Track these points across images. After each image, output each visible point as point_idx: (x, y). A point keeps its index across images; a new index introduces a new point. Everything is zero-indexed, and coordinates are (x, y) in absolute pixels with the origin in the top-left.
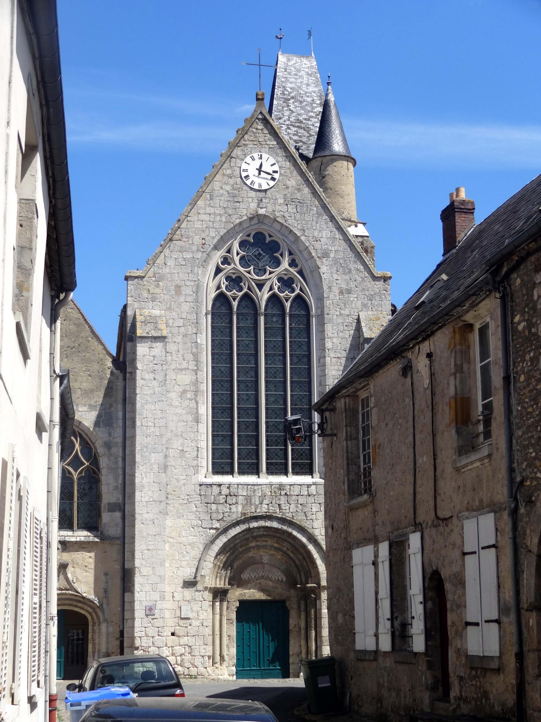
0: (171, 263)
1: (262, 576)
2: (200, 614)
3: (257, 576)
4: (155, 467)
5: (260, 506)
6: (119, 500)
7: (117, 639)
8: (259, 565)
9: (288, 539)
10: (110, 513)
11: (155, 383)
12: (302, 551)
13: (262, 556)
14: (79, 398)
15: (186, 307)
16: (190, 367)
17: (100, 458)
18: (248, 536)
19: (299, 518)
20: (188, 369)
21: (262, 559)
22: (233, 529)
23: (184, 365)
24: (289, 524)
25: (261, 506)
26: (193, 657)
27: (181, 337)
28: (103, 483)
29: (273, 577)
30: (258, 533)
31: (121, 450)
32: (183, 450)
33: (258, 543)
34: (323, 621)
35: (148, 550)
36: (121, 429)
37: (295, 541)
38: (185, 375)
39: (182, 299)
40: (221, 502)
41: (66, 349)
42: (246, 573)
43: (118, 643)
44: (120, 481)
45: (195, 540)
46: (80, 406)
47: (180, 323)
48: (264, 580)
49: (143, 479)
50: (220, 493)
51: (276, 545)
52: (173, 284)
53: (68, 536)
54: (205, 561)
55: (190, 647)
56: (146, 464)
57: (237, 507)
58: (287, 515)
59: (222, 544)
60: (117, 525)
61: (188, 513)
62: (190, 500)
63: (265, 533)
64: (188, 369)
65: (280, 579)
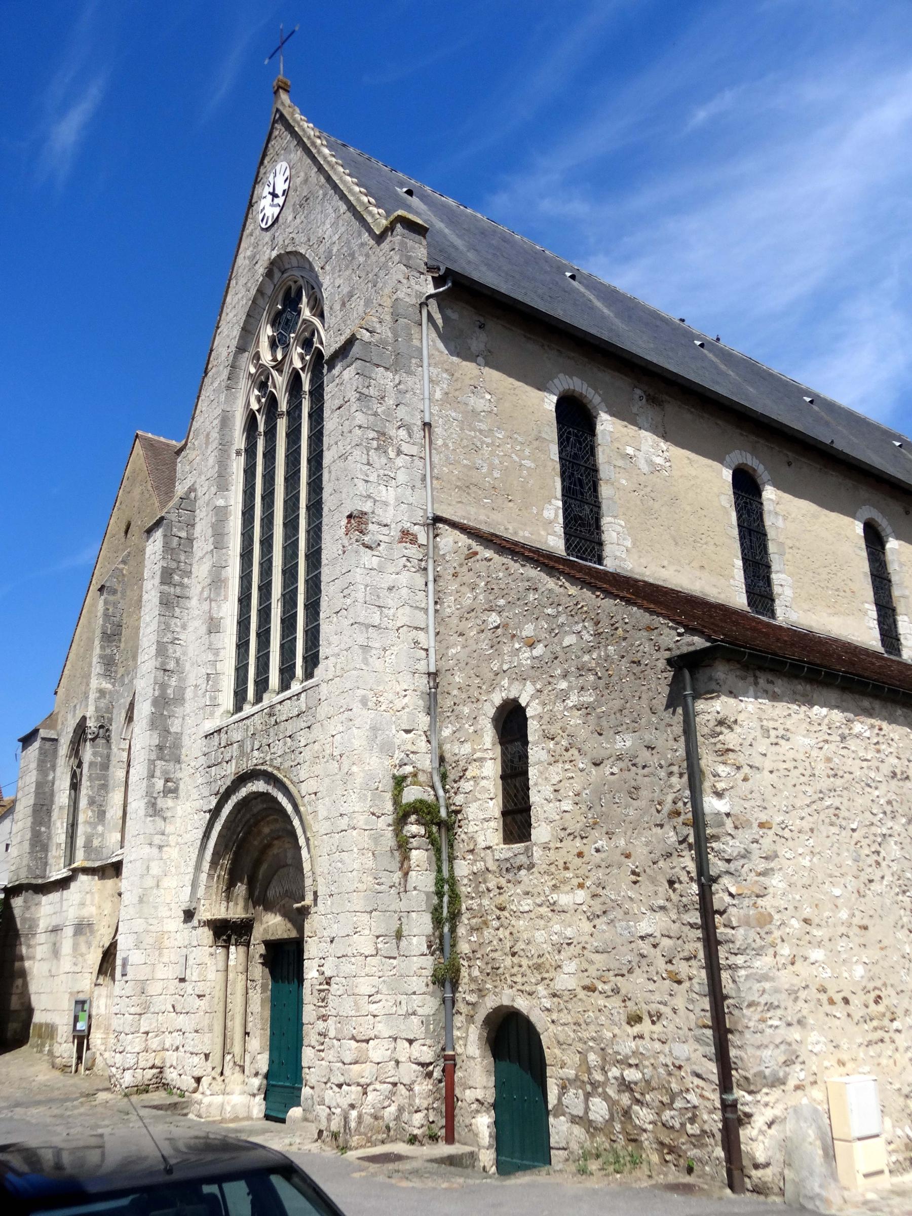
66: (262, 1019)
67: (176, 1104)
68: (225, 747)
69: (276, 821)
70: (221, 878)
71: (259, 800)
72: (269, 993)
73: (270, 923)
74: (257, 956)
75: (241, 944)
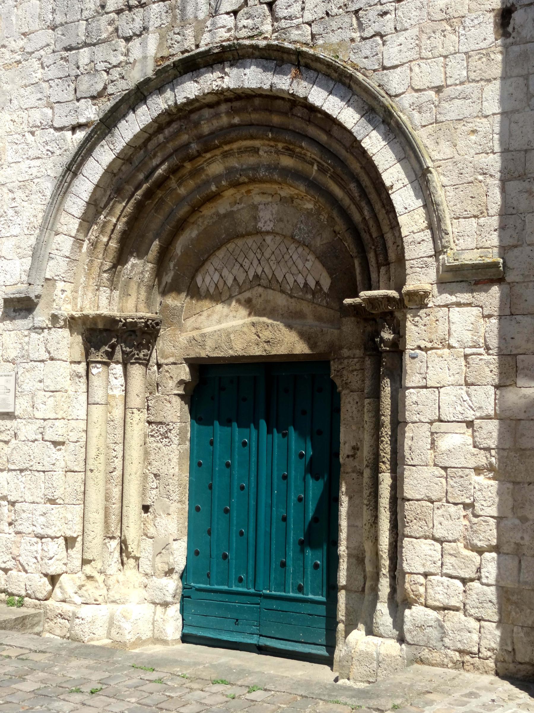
1: (257, 277)
2: (38, 401)
3: (241, 279)
5: (208, 23)
8: (250, 241)
9: (312, 131)
12: (355, 166)
13: (255, 207)
18: (185, 138)
19: (334, 39)
21: (256, 219)
22: (131, 116)
24: (298, 66)
25: (214, 24)
26: (18, 538)
29: (291, 279)
30: (216, 124)
33: (233, 162)
34: (408, 434)
37: (328, 133)
40: (104, 36)
42: (211, 269)
45: (34, 171)
48: (260, 290)
50: (103, 7)
51: (287, 161)
54: (57, 234)
55: (13, 504)
57: (144, 45)
58: (295, 34)
59: (101, 171)
61: (22, 91)
62: (28, 50)
63: (236, 120)
65: (312, 284)
66: (180, 485)
67: (24, 618)
68: (119, 12)
69: (255, 150)
70: (101, 248)
71: (223, 107)
72: (188, 443)
73: (206, 330)
74: (171, 384)
75: (138, 361)
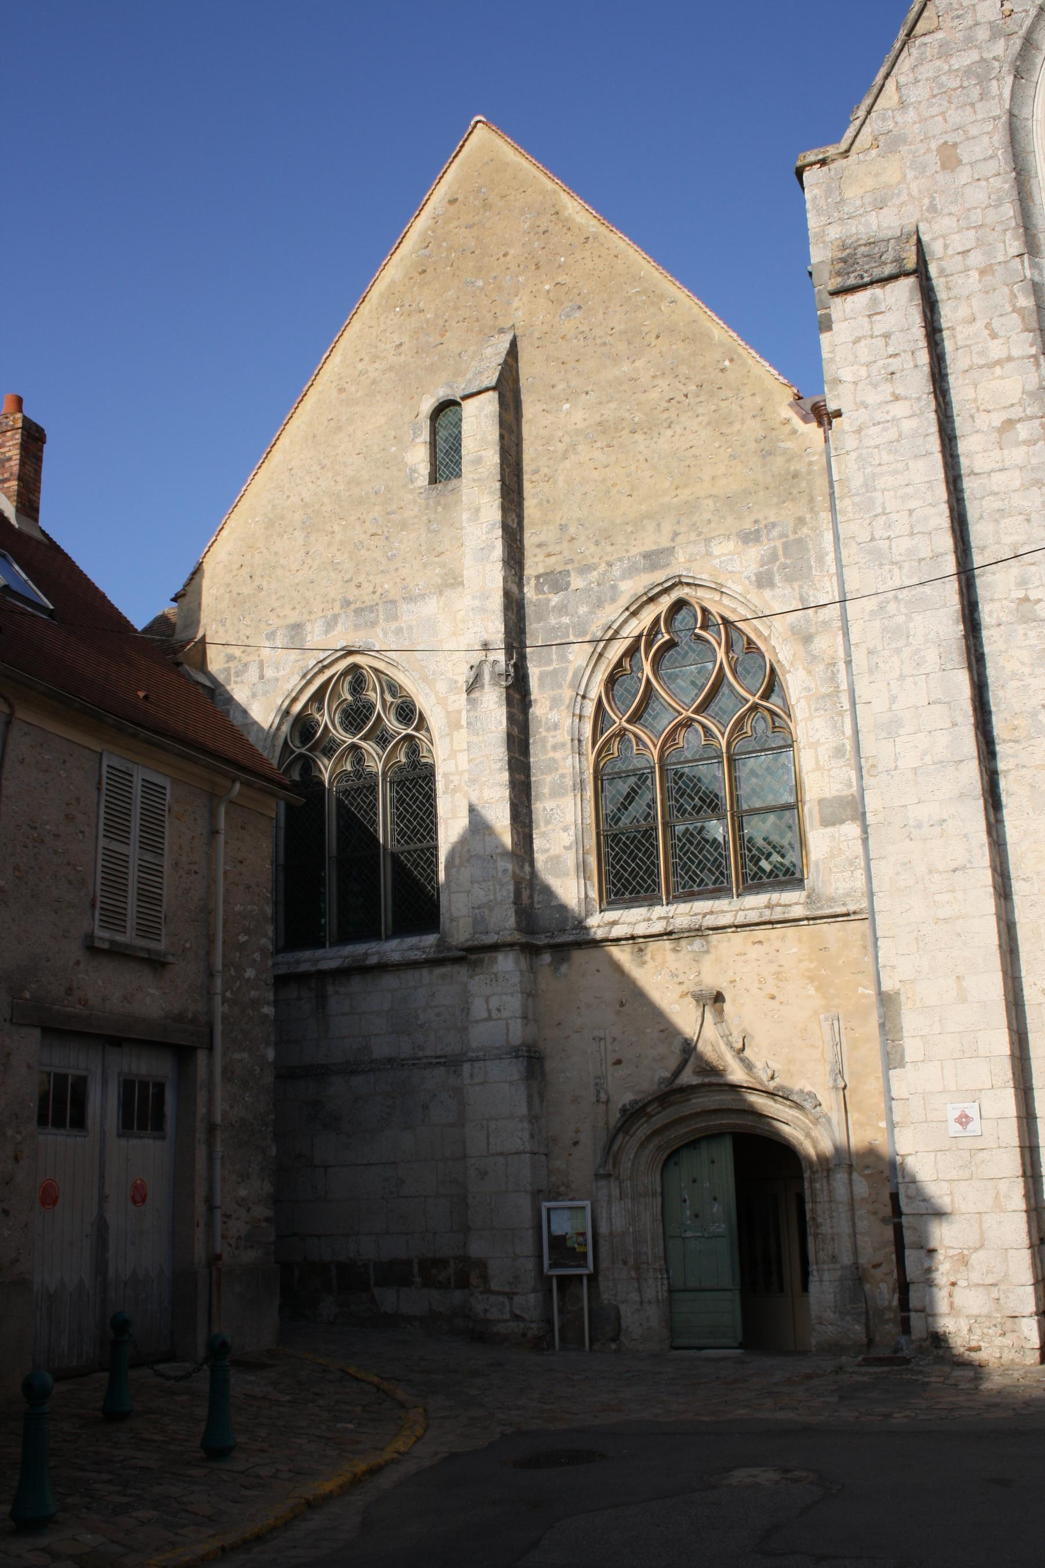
0: (916, 94)
4: (931, 656)
6: (850, 786)
7: (884, 1221)
10: (830, 830)
11: (899, 409)
14: (709, 521)
15: (978, 195)
16: (1016, 352)
17: (788, 676)
20: (1010, 359)
23: (996, 350)
27: (974, 275)
28: (801, 745)
31: (840, 639)
32: (1026, 599)
35: (937, 921)
36: (835, 578)
38: (1002, 378)
39: (964, 175)
41: (666, 405)
43: (889, 1232)
44: (848, 731)
46: (714, 542)
47: (968, 239)
49: (893, 699)
52: (934, 145)
53: (712, 913)
56: (898, 651)
60: (851, 863)
64: (1010, 359)
